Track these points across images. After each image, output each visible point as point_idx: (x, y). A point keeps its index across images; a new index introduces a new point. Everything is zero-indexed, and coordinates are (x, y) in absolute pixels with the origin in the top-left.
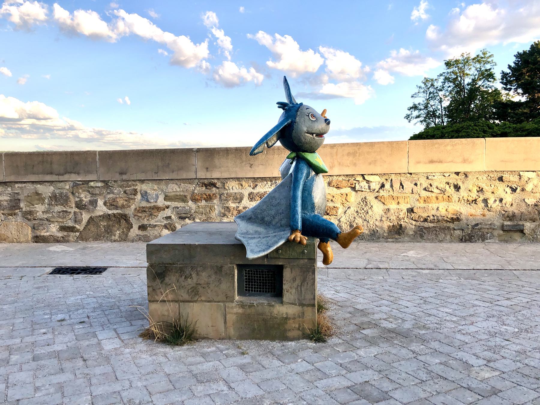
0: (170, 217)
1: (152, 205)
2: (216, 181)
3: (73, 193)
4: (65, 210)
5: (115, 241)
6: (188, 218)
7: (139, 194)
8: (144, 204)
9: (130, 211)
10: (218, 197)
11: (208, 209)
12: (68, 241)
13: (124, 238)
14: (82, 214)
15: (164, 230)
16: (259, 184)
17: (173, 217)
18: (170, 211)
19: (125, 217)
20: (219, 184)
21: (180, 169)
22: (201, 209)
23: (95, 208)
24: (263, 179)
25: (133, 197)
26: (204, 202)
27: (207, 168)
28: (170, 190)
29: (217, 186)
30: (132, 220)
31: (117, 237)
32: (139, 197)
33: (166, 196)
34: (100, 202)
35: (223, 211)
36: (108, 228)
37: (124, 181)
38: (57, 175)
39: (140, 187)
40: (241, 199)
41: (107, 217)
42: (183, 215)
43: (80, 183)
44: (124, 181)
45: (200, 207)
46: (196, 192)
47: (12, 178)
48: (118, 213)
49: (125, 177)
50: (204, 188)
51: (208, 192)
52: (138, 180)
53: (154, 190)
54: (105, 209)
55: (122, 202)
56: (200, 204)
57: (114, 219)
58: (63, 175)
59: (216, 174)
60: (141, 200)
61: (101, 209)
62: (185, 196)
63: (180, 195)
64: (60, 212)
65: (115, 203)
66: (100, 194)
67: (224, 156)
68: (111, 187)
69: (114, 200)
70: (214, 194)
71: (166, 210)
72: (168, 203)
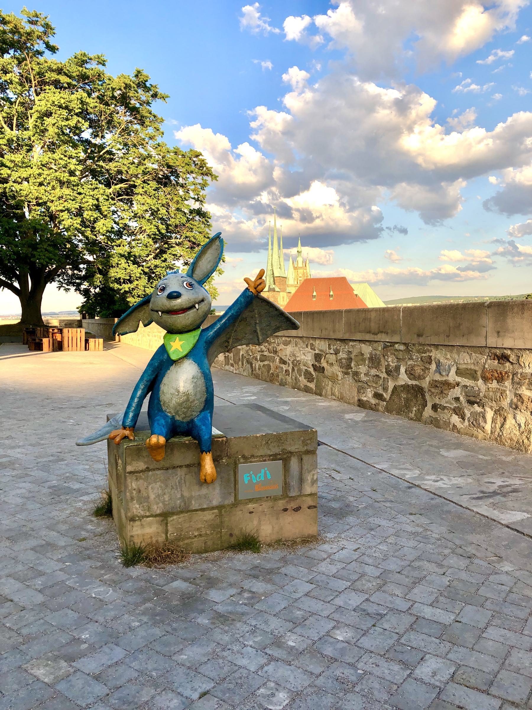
0: (457, 399)
1: (444, 379)
2: (509, 352)
3: (384, 356)
4: (378, 374)
5: (411, 419)
6: (477, 403)
7: (433, 362)
8: (437, 377)
9: (425, 384)
10: (511, 377)
11: (499, 395)
12: (377, 410)
13: (418, 418)
14: (388, 381)
15: (454, 415)
18: (460, 390)
19: (419, 391)
20: (513, 358)
21: (470, 332)
23: (399, 374)
26: (495, 382)
27: (498, 332)
28: (462, 362)
30: (427, 397)
32: (433, 367)
33: (458, 369)
34: (403, 370)
36: (407, 402)
37: (421, 344)
38: (373, 334)
39: (435, 354)
41: (406, 387)
42: (472, 399)
43: (389, 344)
44: (421, 344)
45: (490, 389)
46: (487, 366)
48: (416, 385)
49: (421, 340)
51: (500, 368)
53: (447, 359)
55: (419, 371)
56: (490, 385)
59: (508, 343)
60: (436, 371)
61: (403, 379)
62: (476, 371)
63: (471, 369)
64: (374, 376)
65: (412, 372)
66: (403, 360)
67: (517, 313)
68: (411, 351)
72: (459, 379)
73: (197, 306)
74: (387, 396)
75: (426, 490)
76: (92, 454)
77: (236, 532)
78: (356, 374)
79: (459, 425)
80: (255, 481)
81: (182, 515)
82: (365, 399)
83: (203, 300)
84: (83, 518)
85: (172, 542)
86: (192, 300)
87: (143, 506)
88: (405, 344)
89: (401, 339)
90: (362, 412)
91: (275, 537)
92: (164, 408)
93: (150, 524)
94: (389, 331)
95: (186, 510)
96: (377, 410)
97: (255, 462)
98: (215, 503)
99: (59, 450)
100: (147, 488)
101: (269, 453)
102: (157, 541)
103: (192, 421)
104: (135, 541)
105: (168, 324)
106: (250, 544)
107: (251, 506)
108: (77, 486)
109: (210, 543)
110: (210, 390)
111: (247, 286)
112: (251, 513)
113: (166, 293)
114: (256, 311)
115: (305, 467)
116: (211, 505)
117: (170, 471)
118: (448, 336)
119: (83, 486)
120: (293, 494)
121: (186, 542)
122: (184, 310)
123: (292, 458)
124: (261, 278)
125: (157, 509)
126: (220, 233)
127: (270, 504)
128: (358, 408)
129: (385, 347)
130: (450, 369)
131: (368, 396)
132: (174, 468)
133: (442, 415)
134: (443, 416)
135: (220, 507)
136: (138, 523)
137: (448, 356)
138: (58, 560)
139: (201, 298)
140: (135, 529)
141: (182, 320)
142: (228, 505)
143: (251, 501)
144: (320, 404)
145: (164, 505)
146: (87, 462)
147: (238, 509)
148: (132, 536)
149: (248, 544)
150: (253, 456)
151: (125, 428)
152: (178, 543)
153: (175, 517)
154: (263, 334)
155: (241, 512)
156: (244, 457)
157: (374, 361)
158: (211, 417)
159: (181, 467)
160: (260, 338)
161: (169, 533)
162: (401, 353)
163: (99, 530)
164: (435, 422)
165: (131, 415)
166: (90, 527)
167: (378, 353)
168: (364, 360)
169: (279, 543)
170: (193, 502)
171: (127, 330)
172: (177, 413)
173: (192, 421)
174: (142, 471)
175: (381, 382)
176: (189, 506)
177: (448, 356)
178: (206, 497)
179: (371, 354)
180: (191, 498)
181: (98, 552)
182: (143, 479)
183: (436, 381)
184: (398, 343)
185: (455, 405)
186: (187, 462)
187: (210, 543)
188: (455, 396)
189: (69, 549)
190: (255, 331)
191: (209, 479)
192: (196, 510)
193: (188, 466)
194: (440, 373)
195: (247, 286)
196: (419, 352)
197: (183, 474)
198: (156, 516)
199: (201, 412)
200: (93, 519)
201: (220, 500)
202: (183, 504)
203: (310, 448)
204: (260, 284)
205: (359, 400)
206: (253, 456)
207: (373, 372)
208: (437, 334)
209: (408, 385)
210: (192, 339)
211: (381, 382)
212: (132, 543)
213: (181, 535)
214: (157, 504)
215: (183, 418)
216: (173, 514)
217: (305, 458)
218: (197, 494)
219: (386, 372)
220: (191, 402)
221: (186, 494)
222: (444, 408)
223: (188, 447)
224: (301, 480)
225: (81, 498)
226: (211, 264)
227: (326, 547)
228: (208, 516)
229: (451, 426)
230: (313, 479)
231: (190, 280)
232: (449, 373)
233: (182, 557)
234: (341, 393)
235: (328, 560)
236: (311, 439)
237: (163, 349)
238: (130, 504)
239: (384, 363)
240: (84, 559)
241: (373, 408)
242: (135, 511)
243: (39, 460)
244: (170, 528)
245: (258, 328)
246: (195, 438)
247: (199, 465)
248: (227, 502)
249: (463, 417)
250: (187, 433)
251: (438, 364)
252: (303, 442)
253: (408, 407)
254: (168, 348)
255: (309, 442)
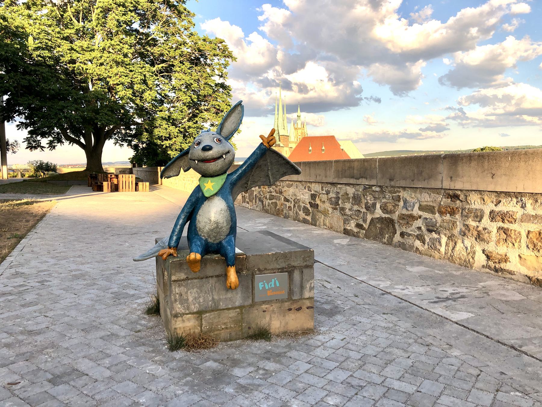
0: (419, 228)
2: (459, 193)
3: (364, 196)
5: (385, 243)
6: (435, 231)
7: (401, 200)
8: (404, 212)
9: (395, 217)
10: (460, 211)
11: (451, 225)
12: (359, 237)
13: (390, 243)
15: (417, 240)
16: (503, 201)
17: (423, 228)
20: (462, 197)
21: (430, 177)
22: (445, 224)
24: (508, 194)
25: (397, 203)
26: (448, 215)
27: (451, 178)
28: (423, 200)
29: (461, 199)
30: (397, 226)
31: (386, 240)
32: (401, 203)
33: (420, 205)
34: (378, 206)
35: (464, 229)
37: (392, 187)
38: (356, 179)
39: (404, 194)
40: (482, 217)
41: (381, 219)
42: (431, 228)
43: (367, 187)
44: (392, 187)
45: (445, 221)
46: (442, 203)
47: (335, 181)
48: (388, 217)
49: (392, 183)
50: (450, 200)
51: (453, 205)
52: (401, 187)
53: (412, 198)
54: (380, 211)
55: (390, 207)
56: (445, 218)
57: (385, 222)
58: (358, 179)
59: (458, 185)
60: (403, 207)
61: (379, 213)
62: (434, 207)
63: (430, 206)
64: (356, 211)
65: (386, 208)
66: (379, 198)
67: (466, 163)
69: (386, 204)
70: (457, 208)
71: (419, 220)
72: (421, 213)
73: (224, 156)
74: (366, 226)
75: (395, 296)
76: (143, 268)
77: (253, 326)
78: (343, 209)
79: (421, 248)
80: (267, 288)
81: (212, 313)
82: (349, 228)
83: (228, 152)
84: (138, 316)
85: (205, 333)
86: (221, 152)
87: (184, 306)
88: (380, 186)
89: (377, 183)
90: (347, 238)
91: (282, 330)
92: (200, 233)
93: (189, 320)
94: (368, 177)
95: (216, 309)
96: (359, 237)
97: (267, 273)
98: (237, 304)
99: (119, 266)
100: (187, 293)
101: (278, 267)
102: (194, 332)
103: (220, 243)
104: (178, 332)
105: (203, 170)
106: (263, 335)
107: (264, 307)
108: (132, 292)
109: (233, 334)
110: (234, 219)
111: (262, 141)
112: (264, 311)
113: (201, 146)
114: (268, 160)
115: (305, 278)
116: (234, 306)
117: (204, 280)
118: (413, 180)
119: (137, 292)
120: (295, 297)
121: (216, 333)
122: (215, 159)
123: (295, 271)
124: (272, 135)
125: (194, 308)
126: (242, 101)
127: (278, 305)
128: (344, 235)
129: (365, 189)
130: (414, 206)
131: (352, 226)
132: (207, 277)
133: (407, 240)
134: (409, 241)
135: (241, 307)
136: (180, 319)
137: (413, 196)
138: (120, 346)
139: (227, 150)
140: (178, 323)
141: (213, 167)
142: (247, 306)
143: (264, 302)
144: (315, 232)
145: (200, 305)
146: (140, 275)
147: (255, 308)
148: (176, 329)
149: (262, 334)
150: (266, 269)
151: (170, 248)
152: (210, 334)
153: (207, 314)
154: (274, 178)
155: (256, 311)
156: (259, 270)
157: (357, 200)
158: (235, 239)
159: (212, 277)
160: (272, 180)
161: (203, 326)
162: (377, 193)
163: (151, 324)
164: (402, 246)
165: (175, 238)
166: (143, 322)
167: (359, 193)
168: (348, 199)
169: (285, 334)
170: (221, 304)
171: (171, 174)
172: (209, 236)
173: (220, 243)
174: (183, 280)
175: (361, 215)
176: (218, 307)
177: (413, 196)
178: (230, 299)
179: (354, 194)
180: (220, 300)
181: (150, 340)
182: (184, 286)
183: (403, 215)
184: (374, 186)
185: (418, 233)
186: (217, 273)
187: (233, 334)
188: (417, 226)
189: (128, 338)
190: (268, 176)
191: (233, 286)
192: (224, 309)
193: (217, 276)
194: (407, 209)
195: (262, 141)
196: (390, 192)
197: (214, 282)
198: (193, 313)
199: (227, 236)
200: (146, 316)
201: (241, 302)
202: (213, 304)
203: (308, 263)
204: (272, 140)
205: (345, 229)
206: (266, 269)
207: (356, 208)
208: (405, 179)
209: (382, 218)
210: (220, 181)
211: (361, 215)
212: (175, 334)
213: (212, 327)
214: (194, 304)
215: (214, 240)
216: (206, 312)
217: (306, 271)
218: (224, 297)
219: (365, 208)
220: (220, 229)
221: (216, 297)
222: (410, 235)
223: (217, 262)
224: (302, 287)
225: (136, 301)
226: (235, 124)
227: (320, 337)
228: (232, 314)
229: (415, 249)
230: (311, 286)
231: (219, 137)
232: (413, 208)
233: (213, 344)
234: (331, 224)
235: (322, 346)
236: (309, 257)
237: (198, 189)
238: (174, 305)
239: (364, 201)
240: (140, 346)
241: (355, 235)
242: (178, 310)
243: (103, 273)
244: (203, 322)
245: (270, 173)
246: (222, 255)
247: (226, 276)
248: (246, 303)
249: (424, 242)
250: (216, 252)
251: (405, 202)
252: (303, 259)
253: (382, 234)
254: (202, 188)
255: (307, 259)
